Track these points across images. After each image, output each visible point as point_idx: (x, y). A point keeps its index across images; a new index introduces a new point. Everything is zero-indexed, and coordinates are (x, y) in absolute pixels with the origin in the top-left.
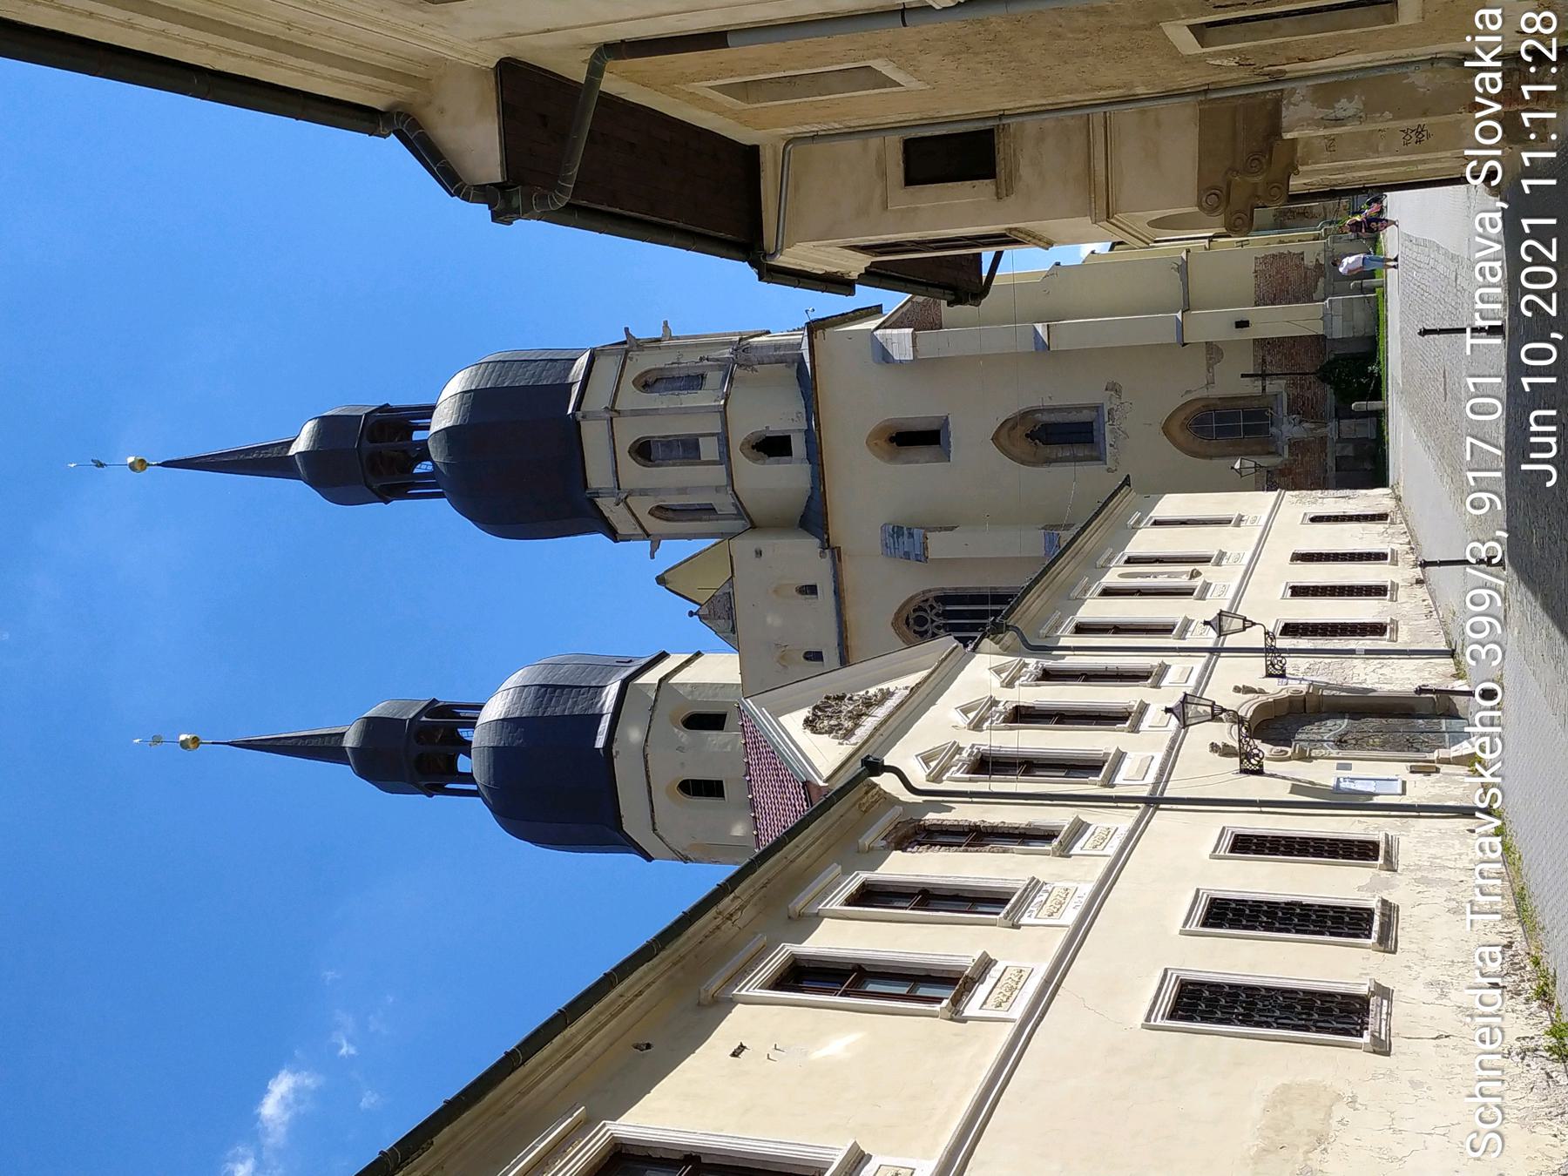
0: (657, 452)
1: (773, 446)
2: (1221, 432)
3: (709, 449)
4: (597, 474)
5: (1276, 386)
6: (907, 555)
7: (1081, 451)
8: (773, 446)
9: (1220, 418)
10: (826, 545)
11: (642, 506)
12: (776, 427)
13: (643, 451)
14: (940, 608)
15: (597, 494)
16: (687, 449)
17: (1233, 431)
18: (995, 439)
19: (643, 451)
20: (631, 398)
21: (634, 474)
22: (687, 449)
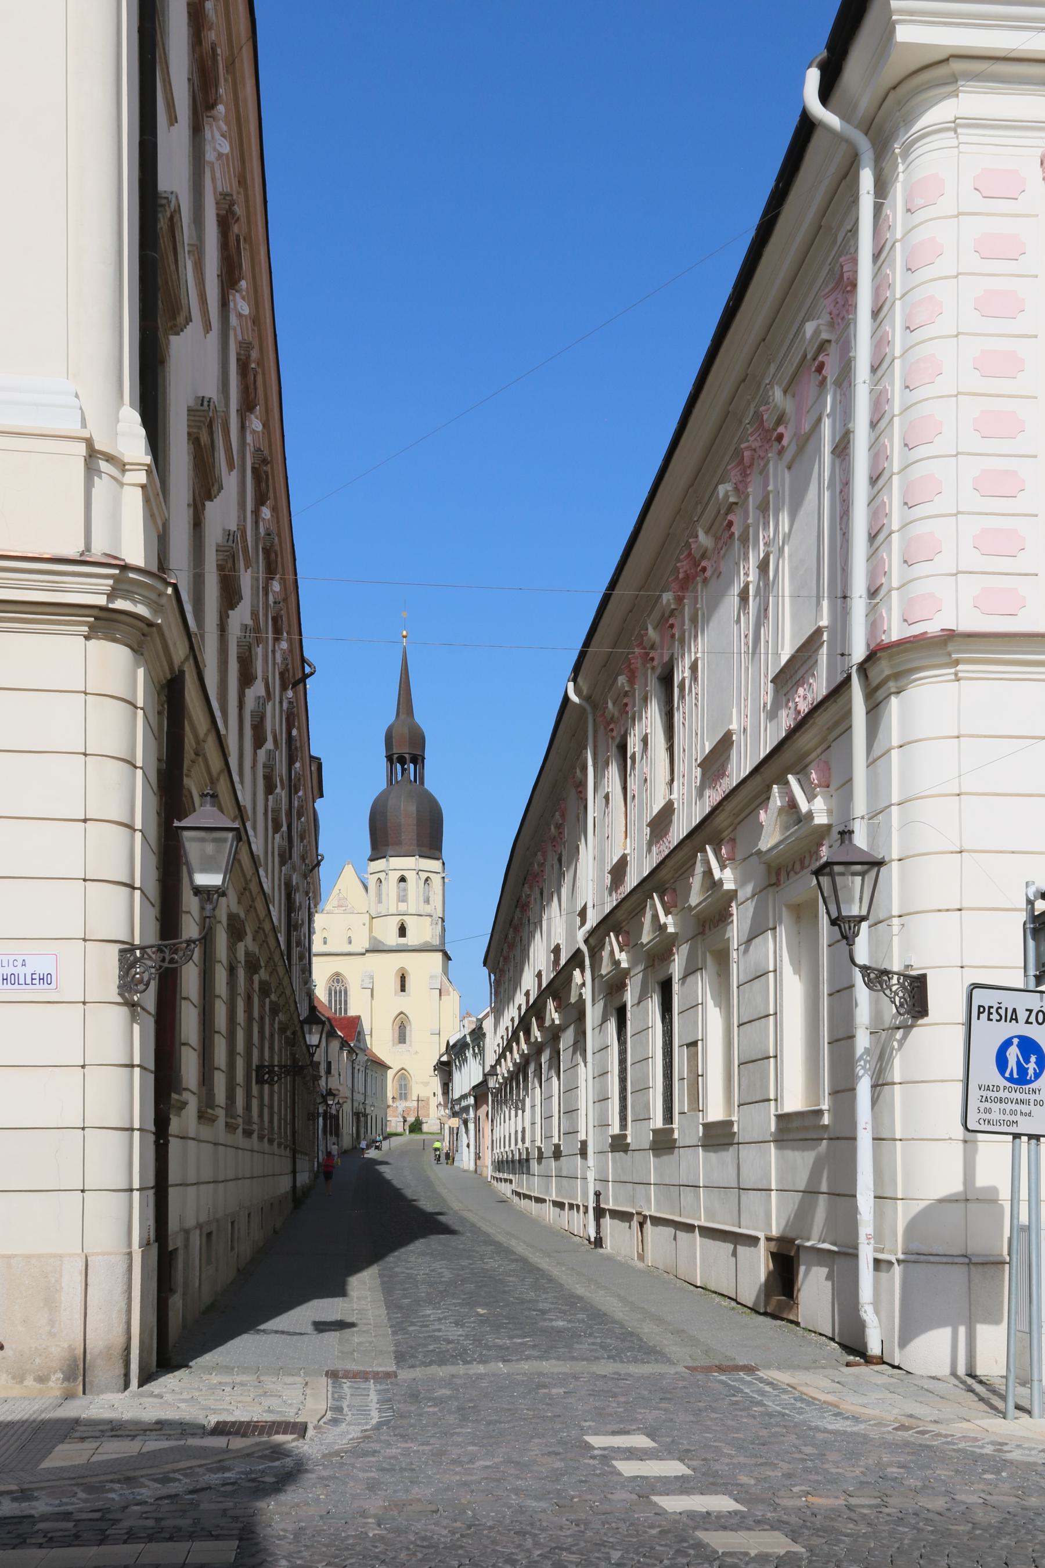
0: (402, 884)
1: (402, 931)
2: (401, 1085)
3: (403, 907)
4: (396, 862)
5: (415, 1104)
6: (363, 981)
7: (397, 1040)
8: (402, 931)
9: (405, 1085)
10: (367, 951)
11: (382, 876)
12: (409, 932)
13: (403, 879)
14: (343, 988)
15: (388, 860)
16: (403, 898)
17: (401, 1089)
18: (402, 1013)
19: (403, 879)
20: (424, 875)
21: (395, 876)
22: (403, 898)
